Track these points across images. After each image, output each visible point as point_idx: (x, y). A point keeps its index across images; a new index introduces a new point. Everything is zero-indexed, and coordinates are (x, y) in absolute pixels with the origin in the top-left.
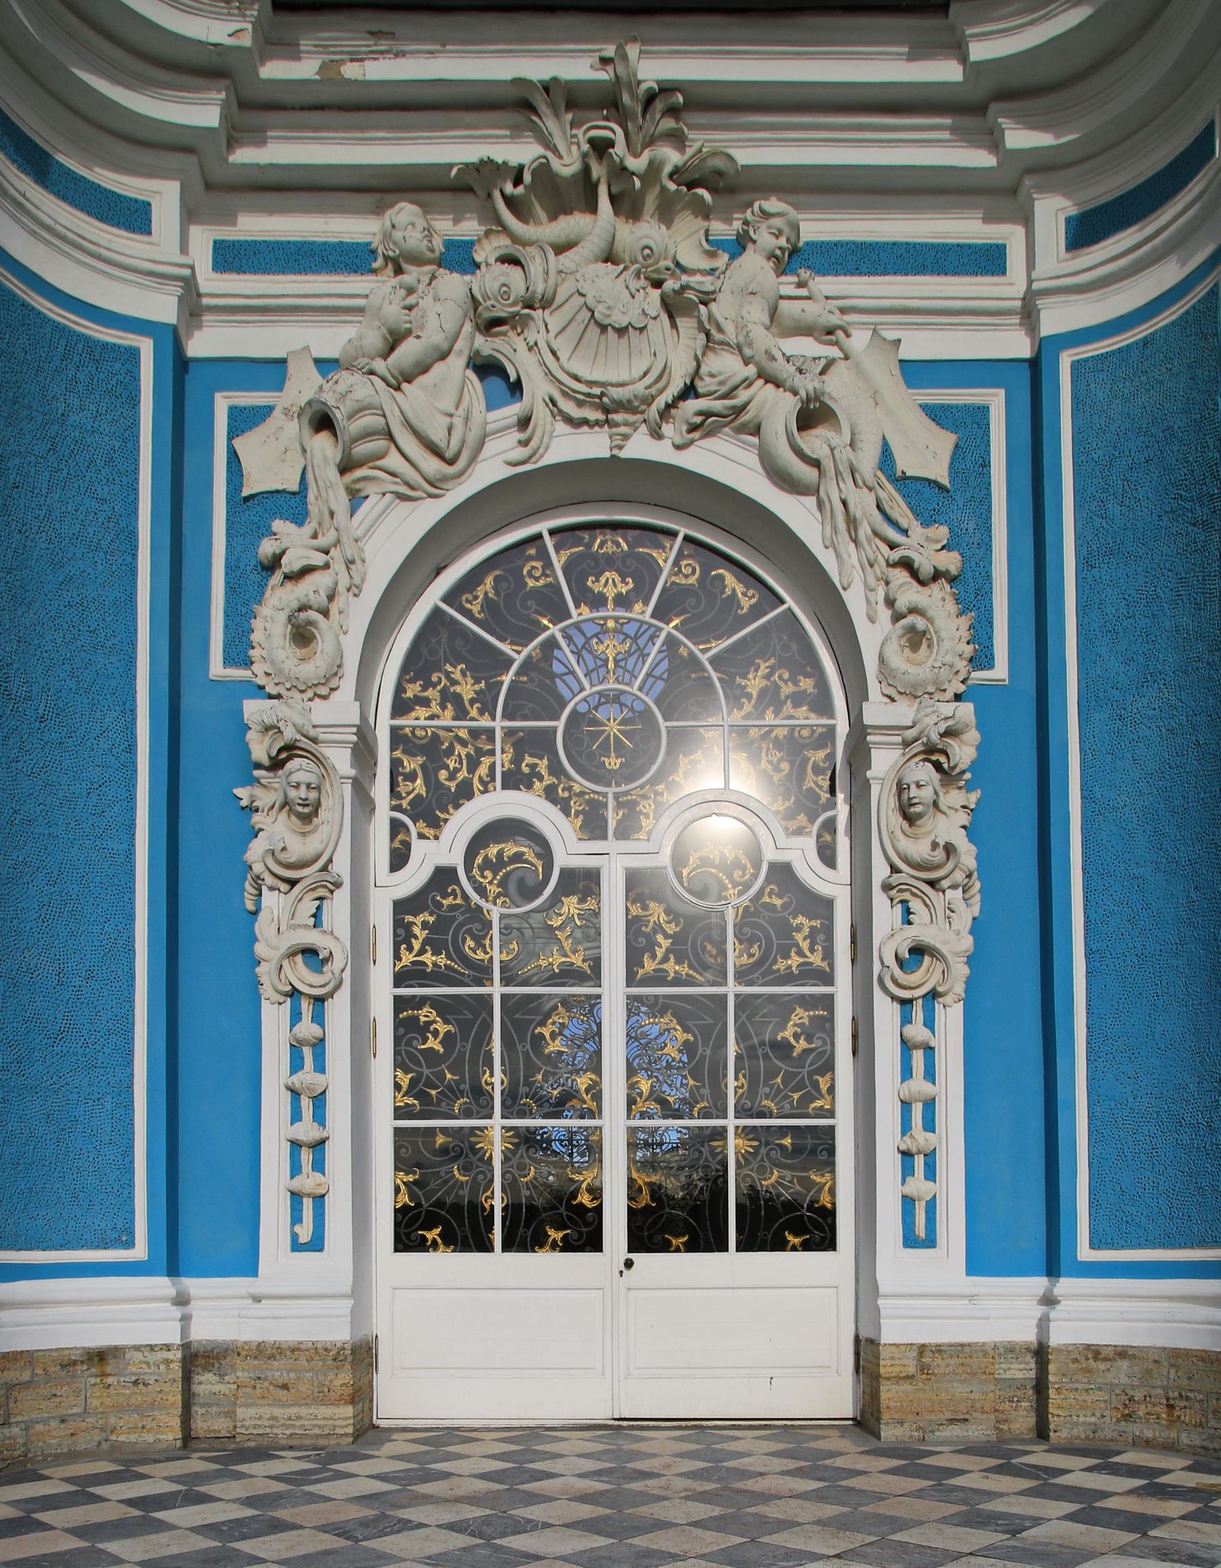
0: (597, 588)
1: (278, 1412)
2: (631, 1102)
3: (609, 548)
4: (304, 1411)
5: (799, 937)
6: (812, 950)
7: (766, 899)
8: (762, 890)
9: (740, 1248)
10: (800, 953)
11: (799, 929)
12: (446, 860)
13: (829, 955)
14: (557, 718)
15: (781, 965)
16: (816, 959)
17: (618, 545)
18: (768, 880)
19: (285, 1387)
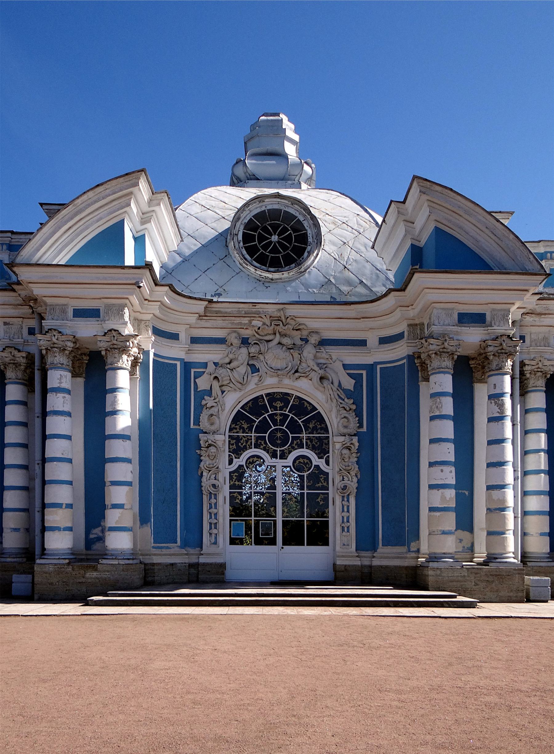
0: (275, 405)
1: (208, 576)
2: (283, 514)
3: (278, 397)
4: (213, 576)
5: (321, 479)
6: (324, 482)
7: (314, 471)
8: (313, 470)
9: (307, 545)
10: (322, 483)
11: (322, 477)
12: (241, 464)
13: (328, 484)
14: (266, 434)
15: (317, 485)
16: (325, 484)
17: (280, 396)
18: (314, 468)
19: (209, 571)
